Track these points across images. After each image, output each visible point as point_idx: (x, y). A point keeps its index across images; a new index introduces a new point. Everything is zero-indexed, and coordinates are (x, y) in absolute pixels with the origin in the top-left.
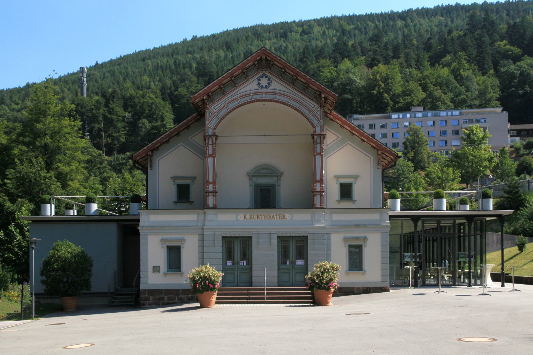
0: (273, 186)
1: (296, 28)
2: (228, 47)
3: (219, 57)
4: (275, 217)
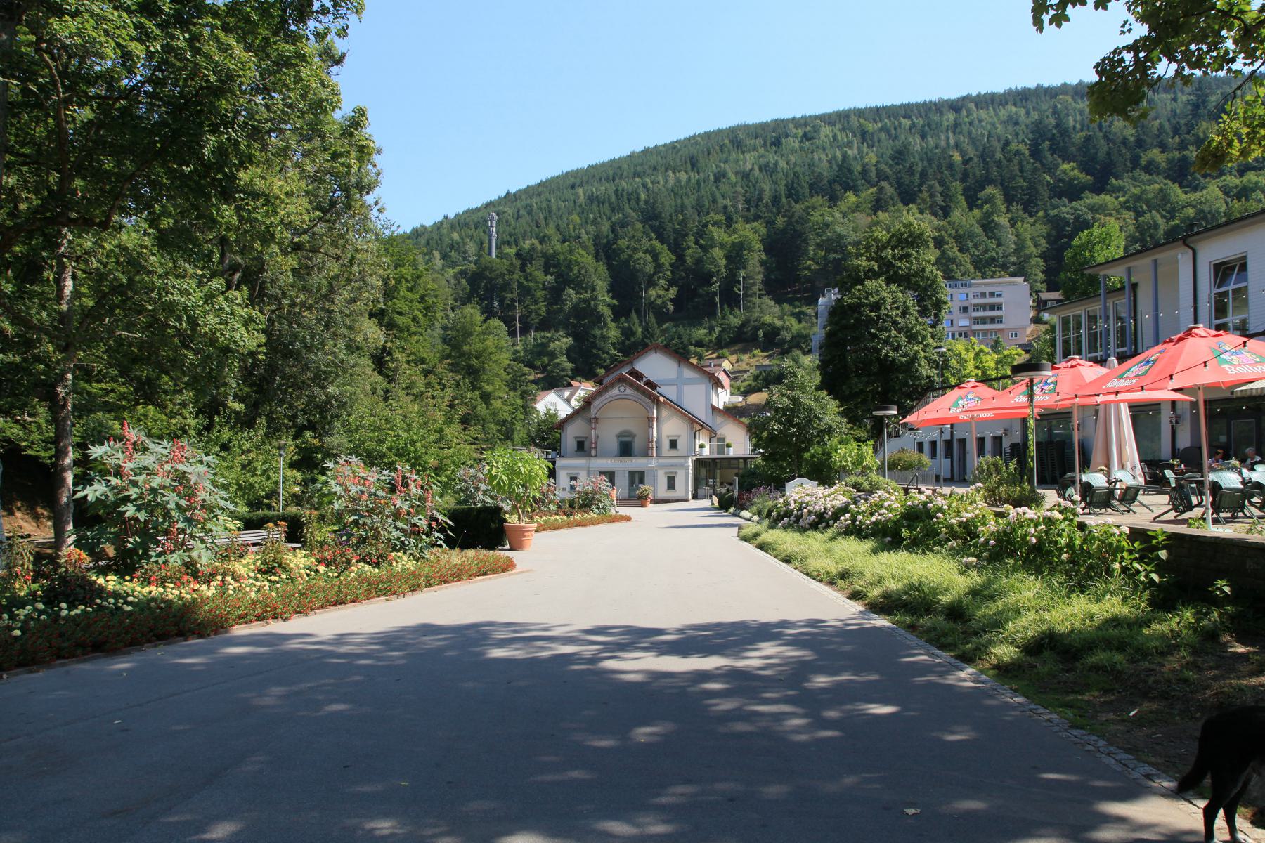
1: (794, 131)
2: (694, 163)
3: (679, 181)
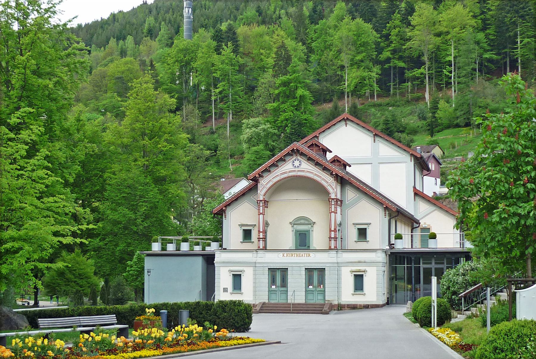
0: (308, 231)
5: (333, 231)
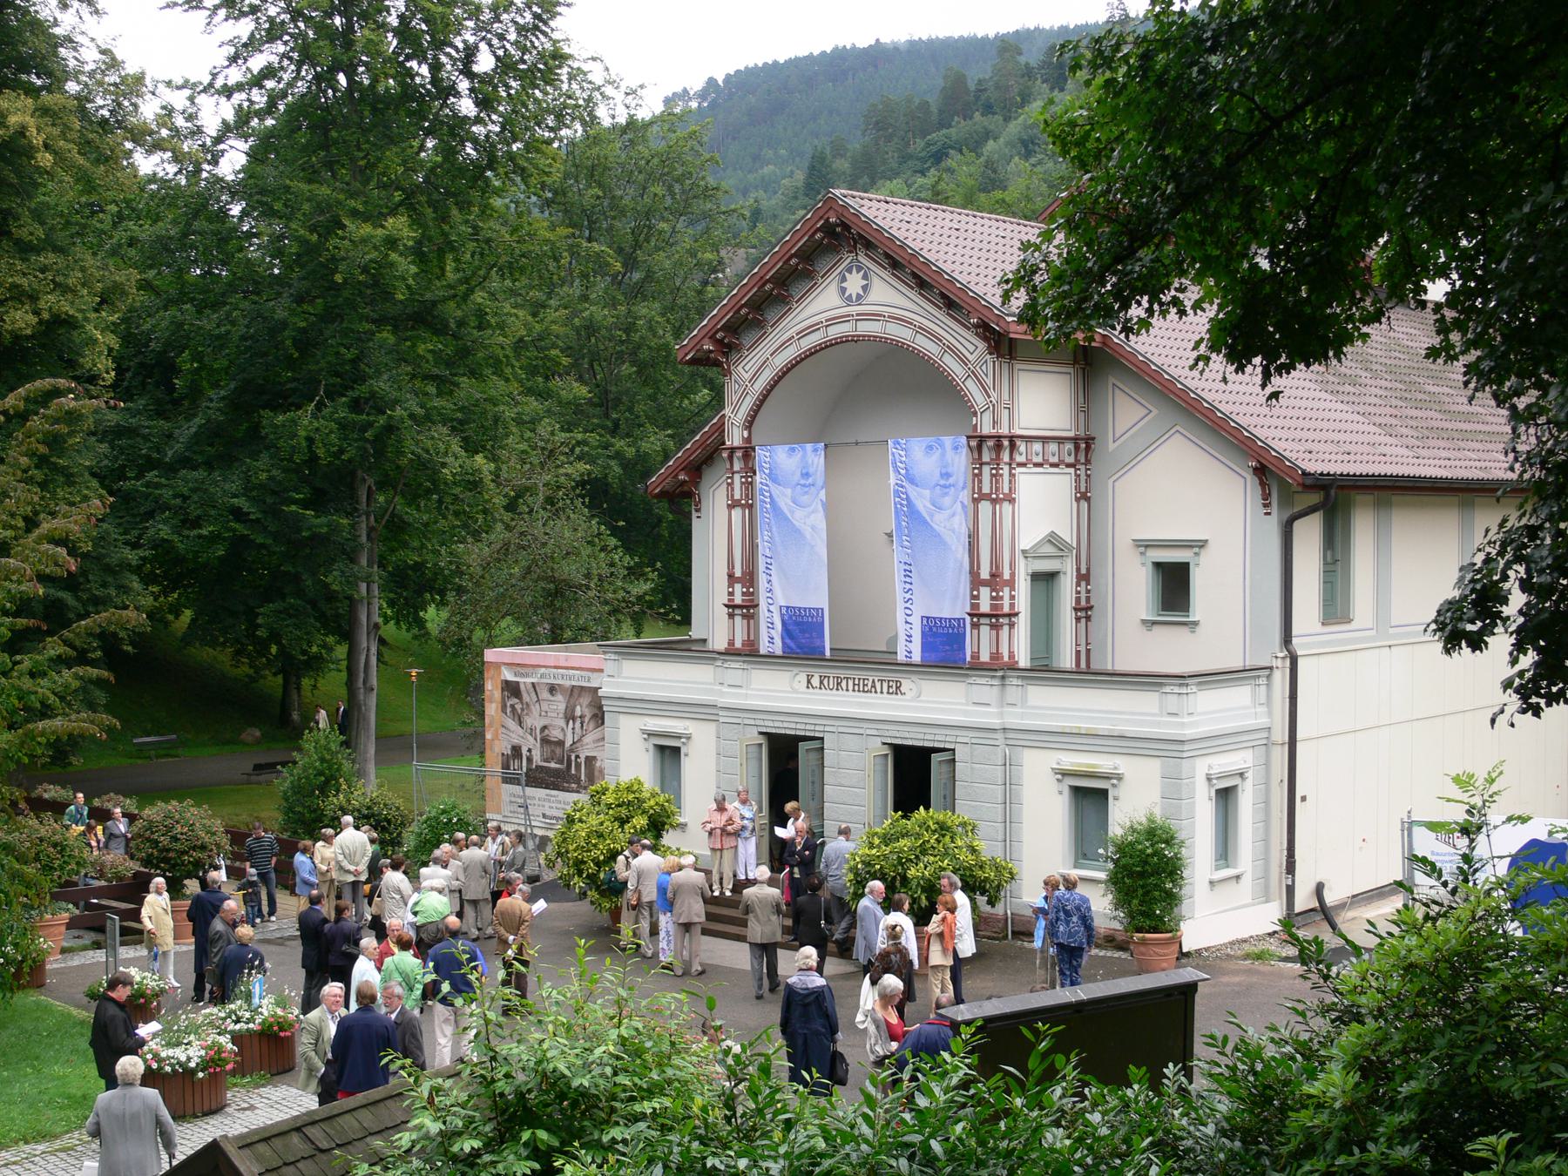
4: (878, 685)
5: (984, 583)
